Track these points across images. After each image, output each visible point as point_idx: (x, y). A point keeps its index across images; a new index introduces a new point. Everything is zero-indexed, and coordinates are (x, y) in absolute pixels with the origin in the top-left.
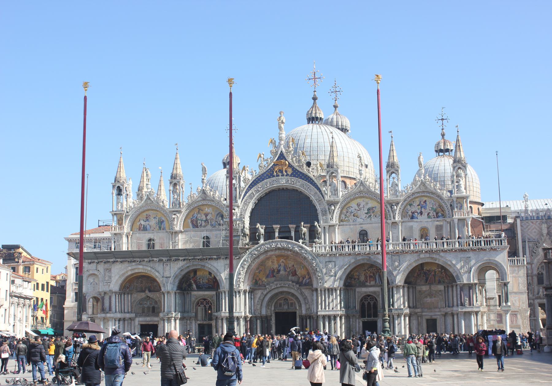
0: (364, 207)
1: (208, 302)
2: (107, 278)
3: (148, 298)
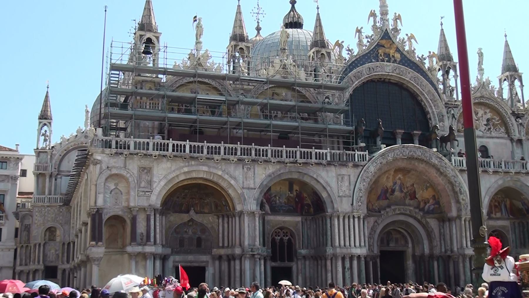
0: (482, 117)
1: (287, 233)
2: (143, 184)
3: (191, 223)
